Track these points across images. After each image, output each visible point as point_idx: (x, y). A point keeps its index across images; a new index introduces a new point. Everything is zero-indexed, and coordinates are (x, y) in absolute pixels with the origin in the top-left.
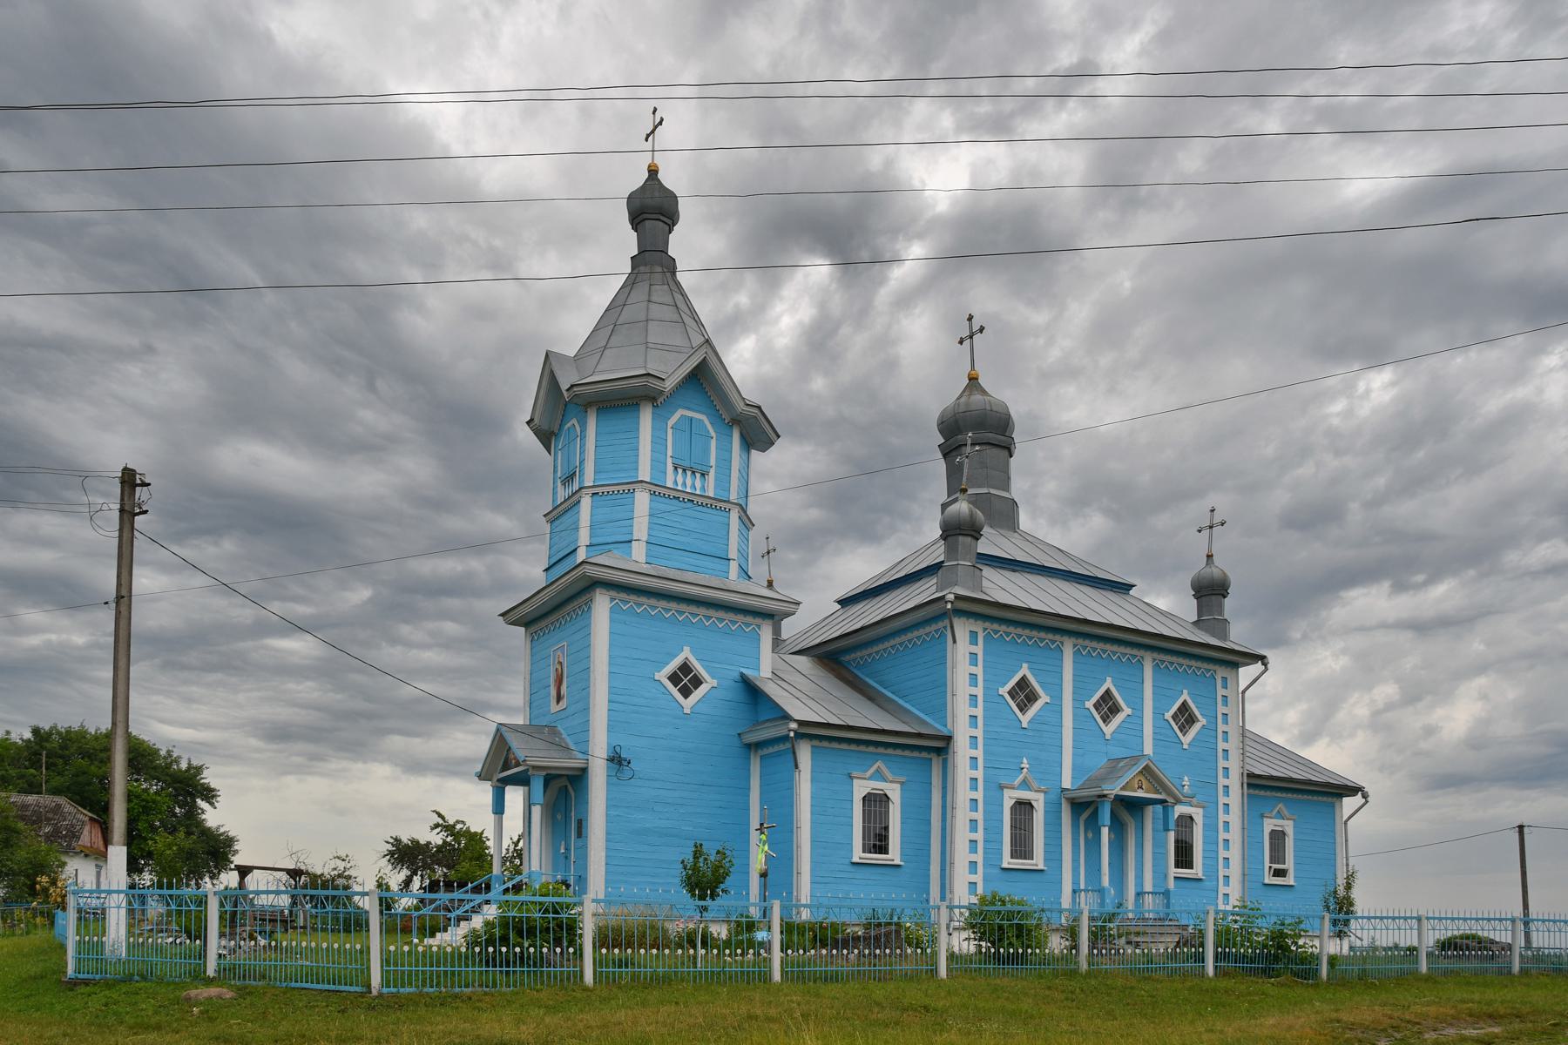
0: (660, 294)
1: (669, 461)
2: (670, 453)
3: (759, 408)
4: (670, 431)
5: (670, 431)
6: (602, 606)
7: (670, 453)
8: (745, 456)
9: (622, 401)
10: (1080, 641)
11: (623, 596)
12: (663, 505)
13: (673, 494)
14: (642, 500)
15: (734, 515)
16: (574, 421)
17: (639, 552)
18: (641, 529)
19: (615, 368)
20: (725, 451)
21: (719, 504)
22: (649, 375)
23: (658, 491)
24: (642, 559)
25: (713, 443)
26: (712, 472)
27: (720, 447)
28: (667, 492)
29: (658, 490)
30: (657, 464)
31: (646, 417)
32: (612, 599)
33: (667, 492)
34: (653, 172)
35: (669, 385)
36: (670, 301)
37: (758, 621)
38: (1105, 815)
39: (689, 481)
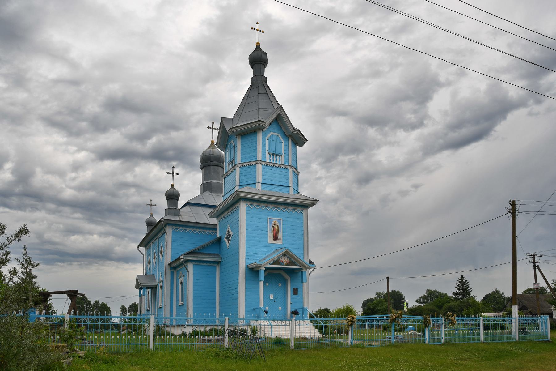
0: (261, 91)
1: (267, 152)
2: (267, 149)
3: (299, 131)
4: (267, 141)
5: (267, 141)
6: (243, 207)
7: (267, 149)
8: (294, 150)
9: (249, 132)
10: (174, 227)
11: (252, 203)
12: (269, 169)
13: (269, 164)
14: (259, 167)
15: (291, 171)
16: (232, 141)
17: (259, 187)
18: (260, 179)
19: (248, 120)
20: (287, 146)
21: (285, 167)
22: (260, 121)
23: (265, 164)
24: (260, 189)
25: (283, 144)
26: (283, 155)
27: (284, 146)
28: (267, 164)
29: (264, 163)
30: (264, 155)
31: (260, 135)
32: (247, 204)
33: (267, 164)
34: (258, 46)
35: (267, 124)
36: (265, 92)
37: (303, 209)
38: (262, 275)
39: (275, 159)
